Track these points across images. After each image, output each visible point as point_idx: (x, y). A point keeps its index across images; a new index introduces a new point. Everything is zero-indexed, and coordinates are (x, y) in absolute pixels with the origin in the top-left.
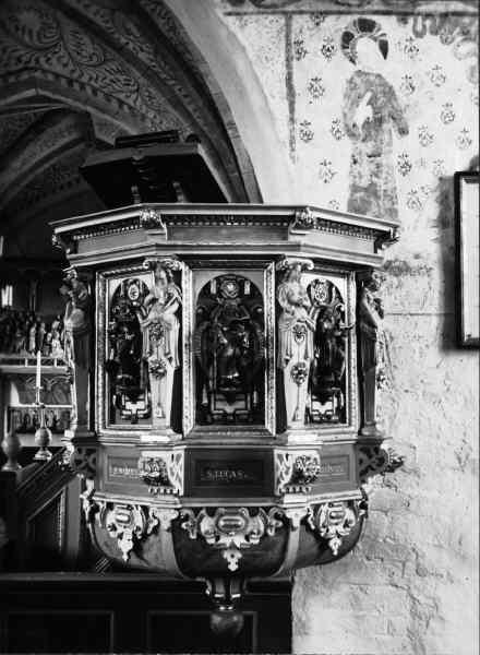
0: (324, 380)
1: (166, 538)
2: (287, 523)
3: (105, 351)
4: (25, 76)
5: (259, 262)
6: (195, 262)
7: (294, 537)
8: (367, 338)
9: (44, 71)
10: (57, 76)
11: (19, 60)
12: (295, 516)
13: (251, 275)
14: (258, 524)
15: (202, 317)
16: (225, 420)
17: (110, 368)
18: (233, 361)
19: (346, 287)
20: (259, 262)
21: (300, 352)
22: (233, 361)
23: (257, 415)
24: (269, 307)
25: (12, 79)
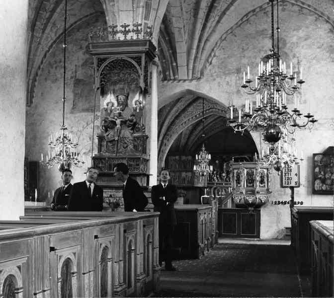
0: (262, 182)
1: (243, 200)
2: (256, 198)
3: (235, 178)
4: (211, 110)
5: (254, 168)
6: (246, 168)
7: (257, 200)
8: (268, 177)
9: (216, 109)
10: (219, 109)
11: (209, 106)
12: (258, 197)
13: (252, 170)
14: (253, 198)
15: (247, 174)
16: (250, 186)
17: (236, 180)
18: (251, 180)
19: (265, 171)
20: (254, 168)
21: (258, 178)
22: (251, 180)
23: (253, 185)
24: (255, 173)
25: (207, 111)
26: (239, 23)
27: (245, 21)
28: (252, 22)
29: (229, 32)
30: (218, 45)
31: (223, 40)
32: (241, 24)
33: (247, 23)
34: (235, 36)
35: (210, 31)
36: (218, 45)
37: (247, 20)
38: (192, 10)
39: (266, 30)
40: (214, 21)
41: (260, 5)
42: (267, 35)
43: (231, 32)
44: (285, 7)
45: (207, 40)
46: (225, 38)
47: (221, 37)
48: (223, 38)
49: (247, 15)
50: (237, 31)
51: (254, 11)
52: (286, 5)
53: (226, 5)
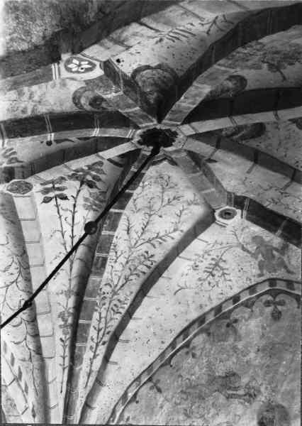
26: (168, 356)
27: (181, 348)
28: (198, 353)
29: (144, 379)
30: (118, 415)
31: (130, 402)
32: (172, 356)
33: (187, 353)
34: (159, 390)
35: (90, 384)
36: (118, 415)
37: (187, 345)
38: (29, 338)
39: (234, 374)
40: (95, 357)
41: (218, 302)
42: (236, 389)
43: (150, 380)
44: (280, 308)
45: (87, 406)
46: (135, 395)
47: (126, 394)
48: (130, 395)
49: (185, 332)
50: (165, 378)
51: (201, 320)
52: (282, 303)
53: (118, 317)
